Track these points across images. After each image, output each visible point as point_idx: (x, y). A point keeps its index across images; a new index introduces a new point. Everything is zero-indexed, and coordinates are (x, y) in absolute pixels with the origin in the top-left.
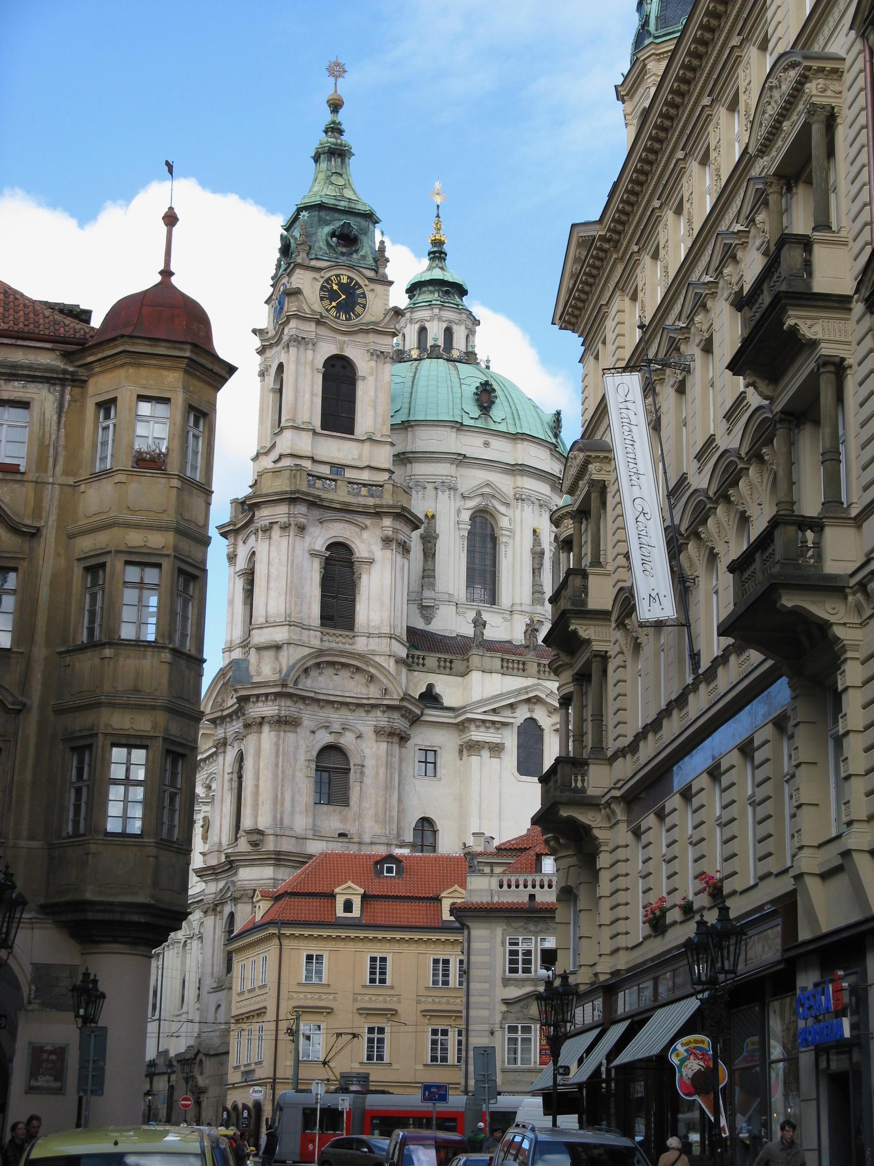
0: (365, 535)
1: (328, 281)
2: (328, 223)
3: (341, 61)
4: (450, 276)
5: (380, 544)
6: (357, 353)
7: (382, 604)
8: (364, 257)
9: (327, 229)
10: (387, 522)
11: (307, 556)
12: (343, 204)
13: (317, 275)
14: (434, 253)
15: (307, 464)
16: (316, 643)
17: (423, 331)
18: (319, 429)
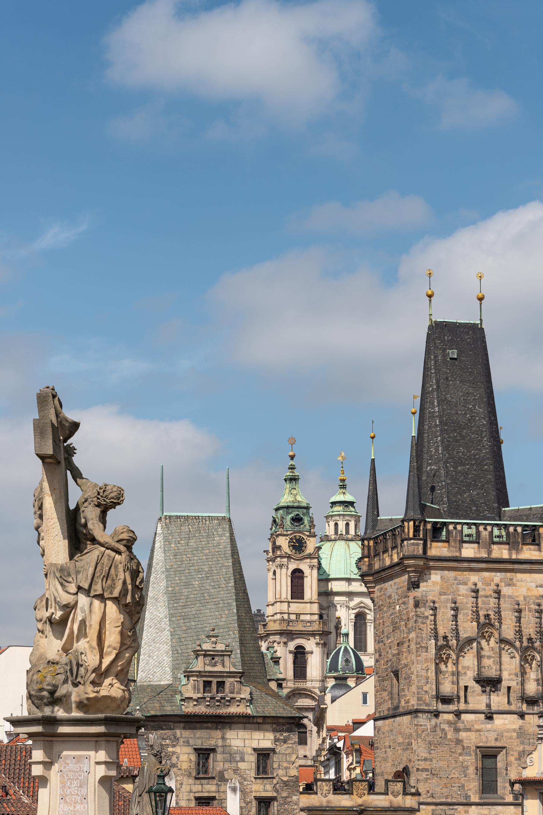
0: (309, 642)
1: (291, 539)
2: (290, 513)
3: (294, 436)
4: (348, 498)
5: (315, 645)
6: (304, 566)
7: (317, 668)
8: (305, 526)
9: (290, 516)
10: (317, 637)
11: (288, 652)
12: (296, 504)
13: (287, 538)
14: (341, 485)
15: (286, 616)
16: (292, 686)
17: (336, 524)
18: (290, 600)
